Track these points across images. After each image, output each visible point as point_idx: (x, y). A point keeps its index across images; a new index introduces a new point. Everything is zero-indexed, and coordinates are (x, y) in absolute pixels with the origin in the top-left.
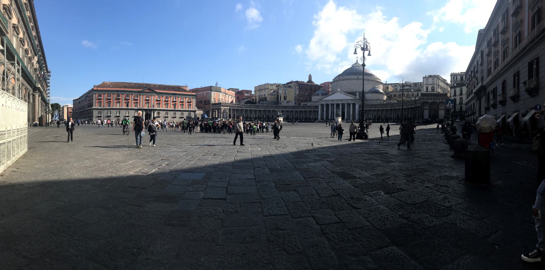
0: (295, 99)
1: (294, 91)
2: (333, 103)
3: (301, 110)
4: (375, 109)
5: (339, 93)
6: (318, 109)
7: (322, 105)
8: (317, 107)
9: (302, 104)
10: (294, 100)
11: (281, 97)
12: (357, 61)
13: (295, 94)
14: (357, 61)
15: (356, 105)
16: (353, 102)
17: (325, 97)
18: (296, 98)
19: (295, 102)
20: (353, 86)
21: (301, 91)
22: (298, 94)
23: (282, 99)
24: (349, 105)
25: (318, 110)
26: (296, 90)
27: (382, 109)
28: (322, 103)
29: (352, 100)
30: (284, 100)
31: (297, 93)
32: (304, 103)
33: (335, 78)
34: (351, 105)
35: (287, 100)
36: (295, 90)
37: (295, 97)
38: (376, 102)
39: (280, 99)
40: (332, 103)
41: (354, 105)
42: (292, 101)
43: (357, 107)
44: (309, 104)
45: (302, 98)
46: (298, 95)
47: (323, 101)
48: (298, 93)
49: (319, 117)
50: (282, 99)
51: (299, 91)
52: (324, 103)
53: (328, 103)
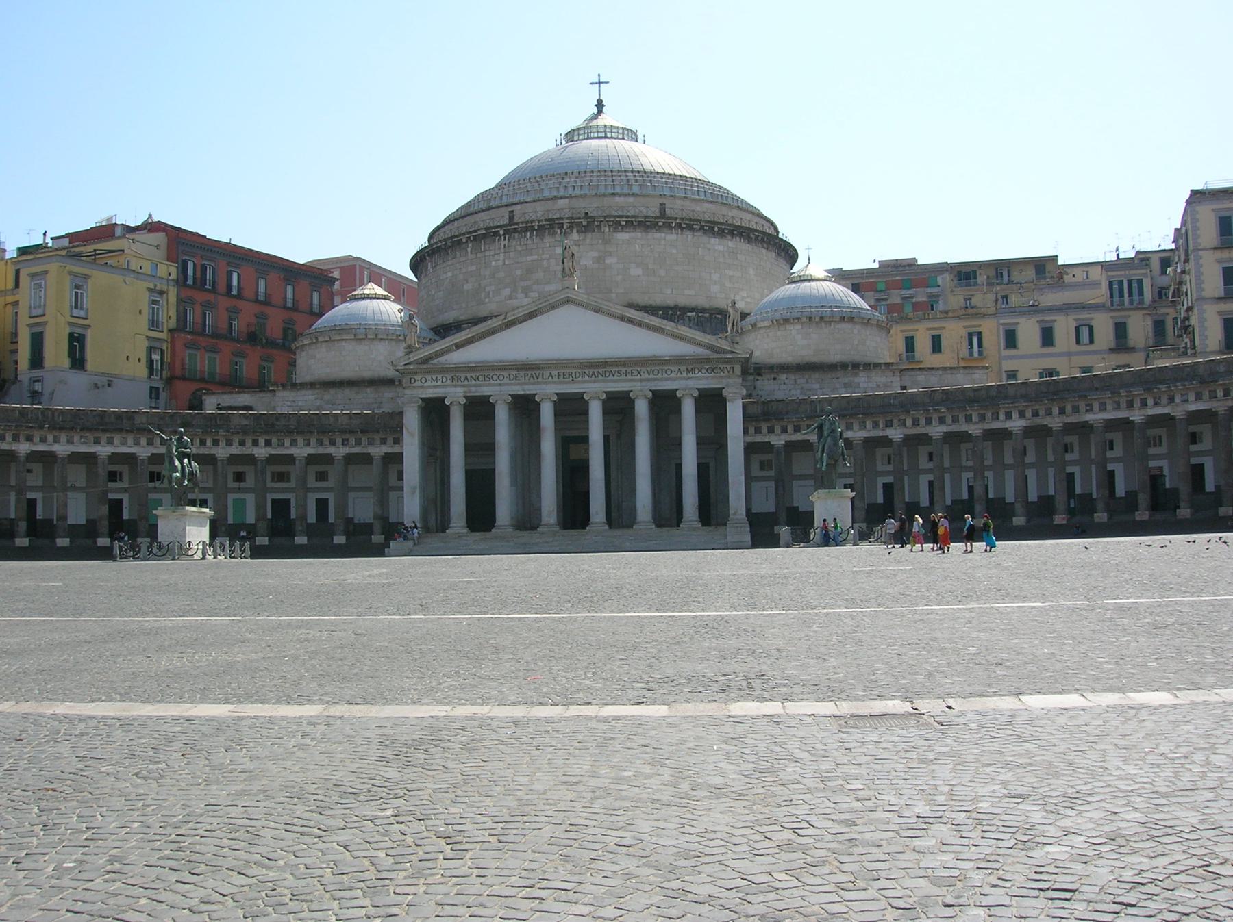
0: (151, 363)
1: (145, 298)
2: (529, 389)
3: (235, 450)
4: (880, 433)
5: (581, 310)
6: (398, 441)
7: (435, 412)
8: (392, 426)
9: (211, 405)
10: (142, 371)
11: (37, 341)
12: (600, 105)
13: (154, 324)
14: (600, 105)
15: (728, 404)
16: (705, 381)
17: (458, 346)
18: (156, 357)
19: (154, 393)
20: (636, 271)
21: (191, 301)
22: (173, 323)
23: (56, 353)
24: (665, 404)
25: (396, 449)
26: (161, 293)
27: (944, 429)
28: (430, 393)
29: (690, 364)
30: (66, 362)
31: (168, 314)
32: (228, 400)
33: (447, 222)
35: (89, 366)
36: (149, 289)
37: (150, 350)
38: (846, 385)
39: (37, 360)
40: (518, 390)
41: (711, 404)
42: (132, 379)
44: (285, 403)
45: (202, 362)
46: (170, 331)
47: (444, 370)
48: (173, 313)
49: (411, 507)
50: (56, 353)
51: (180, 301)
52: (455, 395)
53: (485, 391)
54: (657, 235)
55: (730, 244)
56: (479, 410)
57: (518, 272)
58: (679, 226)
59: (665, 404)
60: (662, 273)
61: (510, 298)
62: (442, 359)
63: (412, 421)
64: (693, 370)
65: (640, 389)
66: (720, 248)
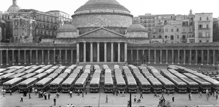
7: (81, 45)
20: (110, 21)
34: (119, 45)
41: (122, 45)
43: (126, 45)
54: (113, 15)
55: (124, 16)
56: (88, 45)
57: (91, 20)
58: (116, 14)
59: (116, 45)
60: (114, 21)
61: (90, 24)
62: (83, 36)
63: (78, 45)
64: (120, 40)
65: (113, 41)
66: (122, 17)
